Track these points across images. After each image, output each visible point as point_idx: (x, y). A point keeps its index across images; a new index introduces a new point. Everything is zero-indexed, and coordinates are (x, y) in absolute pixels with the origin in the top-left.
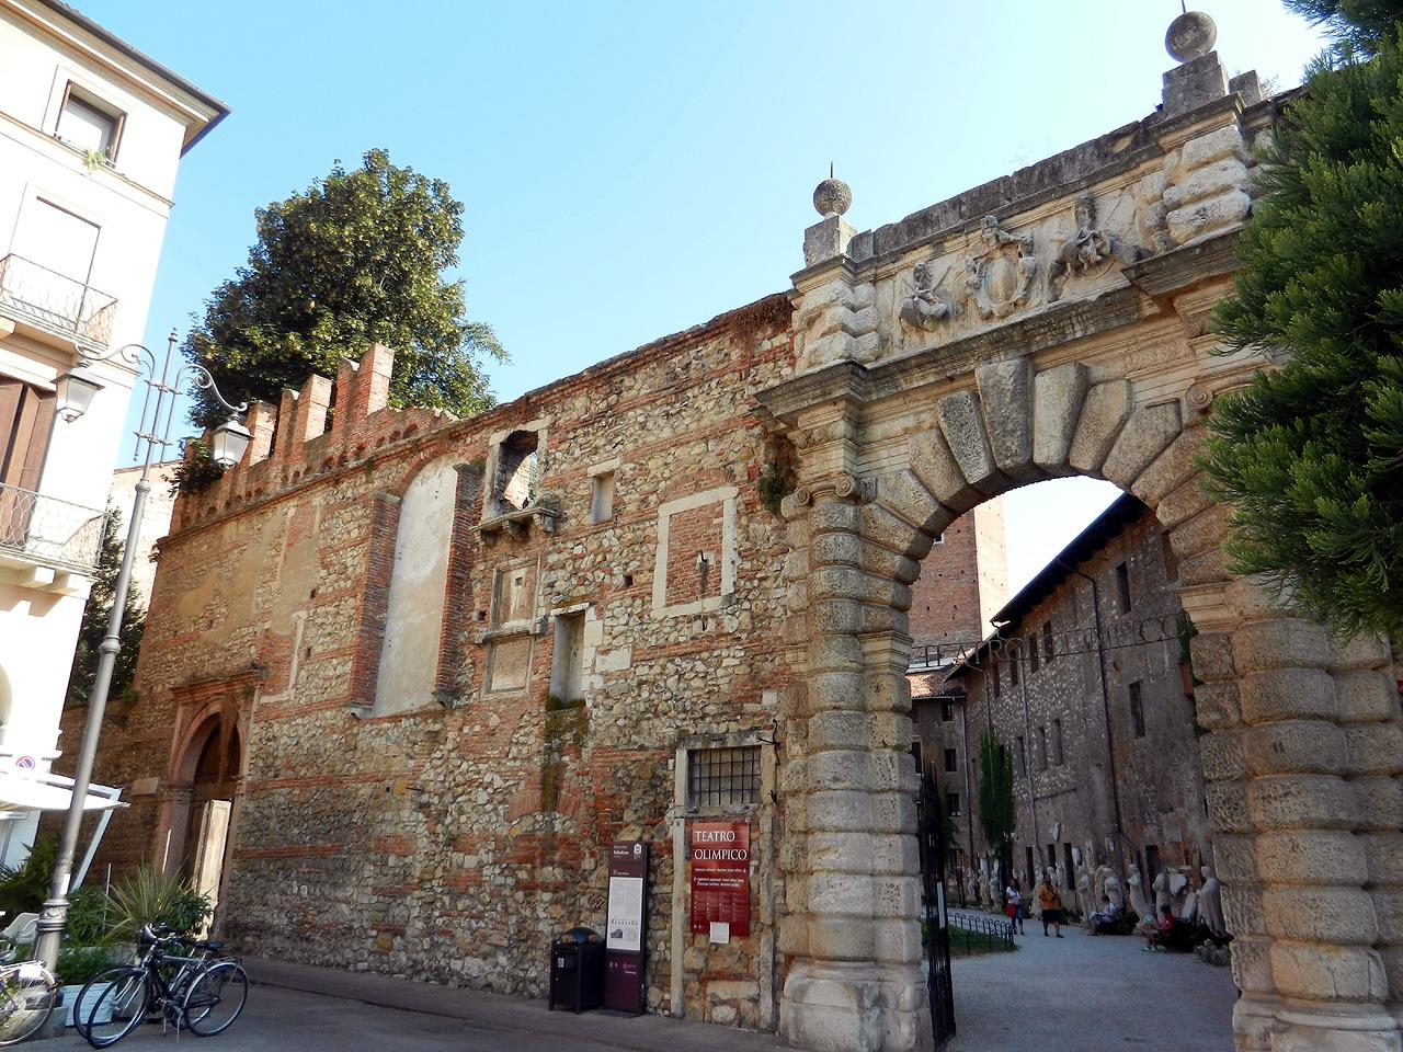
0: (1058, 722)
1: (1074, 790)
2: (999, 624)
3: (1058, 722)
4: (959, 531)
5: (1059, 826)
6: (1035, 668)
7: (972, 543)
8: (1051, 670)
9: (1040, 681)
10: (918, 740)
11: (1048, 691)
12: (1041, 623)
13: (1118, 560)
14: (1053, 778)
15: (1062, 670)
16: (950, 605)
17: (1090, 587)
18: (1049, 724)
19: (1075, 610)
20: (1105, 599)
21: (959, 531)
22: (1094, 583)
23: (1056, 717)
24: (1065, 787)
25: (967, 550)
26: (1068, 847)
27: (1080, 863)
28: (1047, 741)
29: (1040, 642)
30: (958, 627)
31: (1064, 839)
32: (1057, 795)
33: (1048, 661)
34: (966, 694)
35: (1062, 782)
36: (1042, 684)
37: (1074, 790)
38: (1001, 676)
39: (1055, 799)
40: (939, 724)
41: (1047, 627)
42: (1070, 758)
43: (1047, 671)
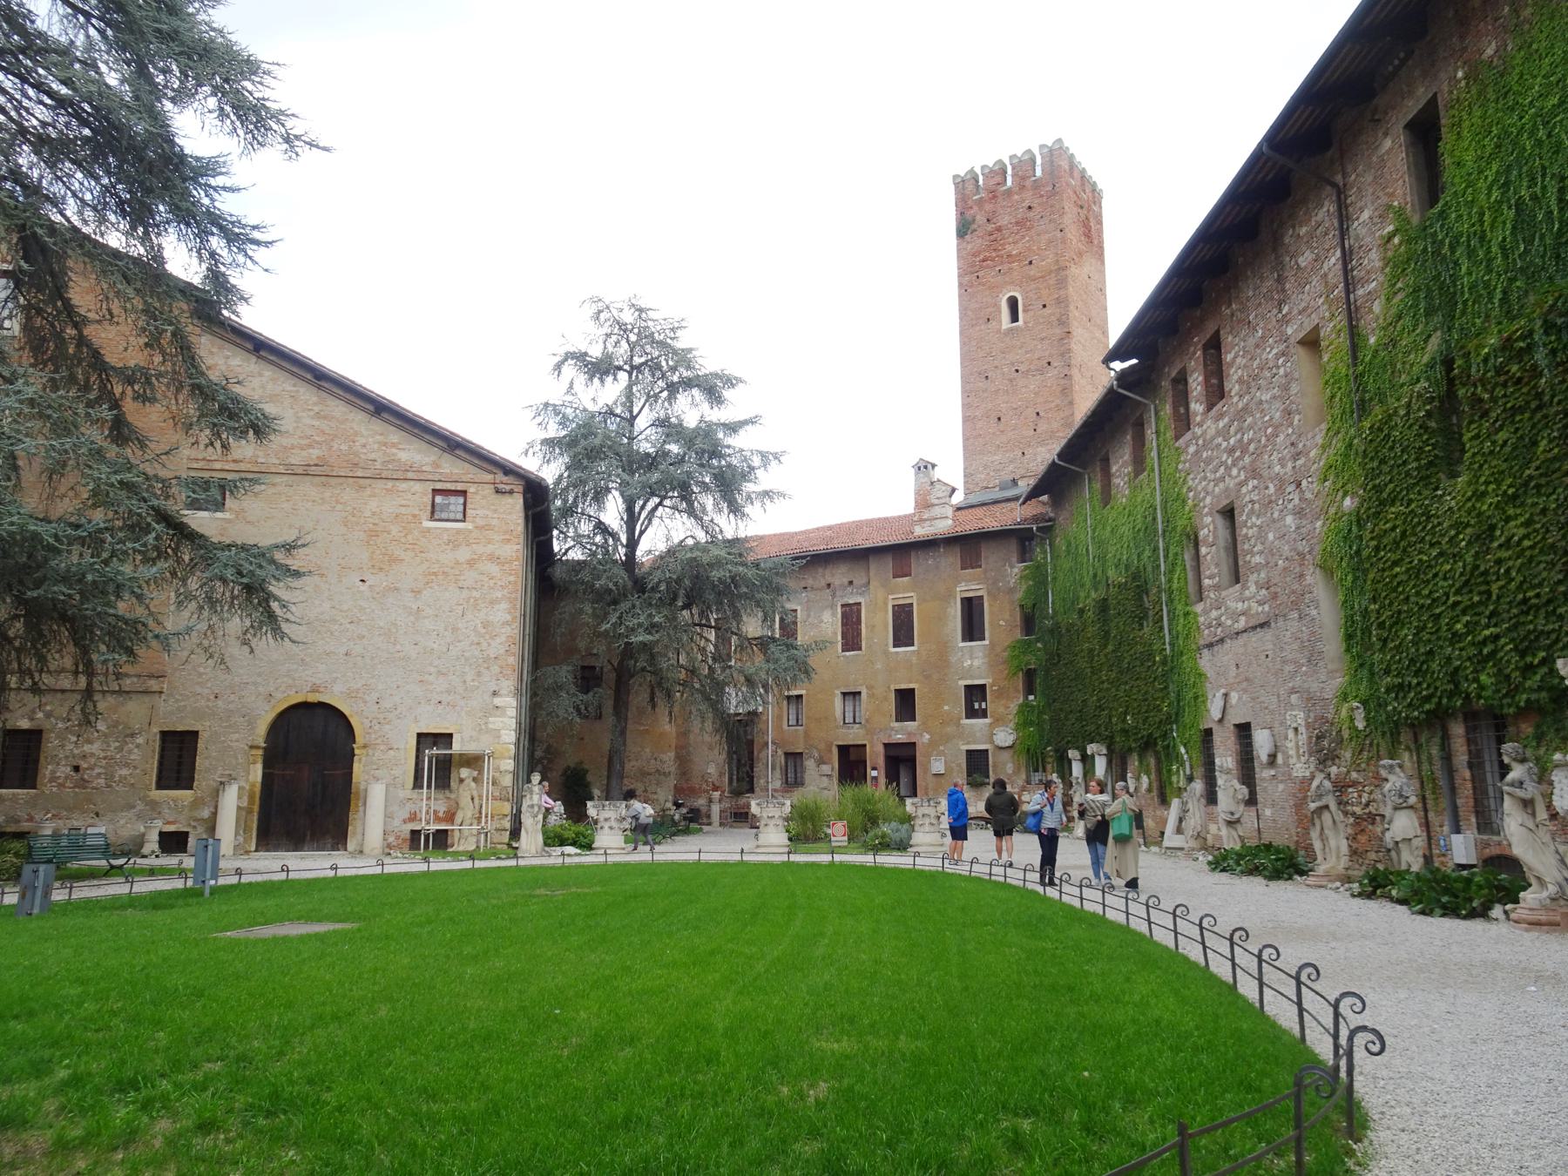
0: (1229, 513)
1: (1262, 626)
2: (1118, 366)
3: (1229, 513)
4: (1044, 306)
5: (1226, 695)
6: (1184, 422)
7: (1063, 322)
8: (1221, 416)
9: (1192, 449)
10: (979, 594)
11: (1208, 461)
12: (1199, 340)
13: (1412, 107)
14: (1214, 614)
15: (1245, 409)
16: (1031, 412)
17: (1329, 206)
18: (1208, 520)
19: (1280, 280)
20: (1365, 215)
21: (1044, 306)
22: (1339, 193)
23: (1225, 502)
24: (1242, 623)
25: (1058, 331)
26: (1244, 730)
27: (1272, 757)
28: (1203, 550)
29: (1196, 383)
30: (1042, 443)
31: (1237, 717)
32: (1222, 641)
33: (1210, 407)
34: (1050, 520)
35: (1236, 616)
36: (1197, 452)
37: (1262, 626)
38: (1114, 469)
39: (1216, 648)
40: (1012, 567)
41: (1214, 346)
42: (1257, 568)
43: (1206, 424)
